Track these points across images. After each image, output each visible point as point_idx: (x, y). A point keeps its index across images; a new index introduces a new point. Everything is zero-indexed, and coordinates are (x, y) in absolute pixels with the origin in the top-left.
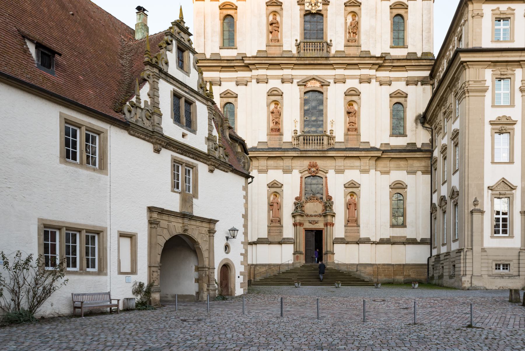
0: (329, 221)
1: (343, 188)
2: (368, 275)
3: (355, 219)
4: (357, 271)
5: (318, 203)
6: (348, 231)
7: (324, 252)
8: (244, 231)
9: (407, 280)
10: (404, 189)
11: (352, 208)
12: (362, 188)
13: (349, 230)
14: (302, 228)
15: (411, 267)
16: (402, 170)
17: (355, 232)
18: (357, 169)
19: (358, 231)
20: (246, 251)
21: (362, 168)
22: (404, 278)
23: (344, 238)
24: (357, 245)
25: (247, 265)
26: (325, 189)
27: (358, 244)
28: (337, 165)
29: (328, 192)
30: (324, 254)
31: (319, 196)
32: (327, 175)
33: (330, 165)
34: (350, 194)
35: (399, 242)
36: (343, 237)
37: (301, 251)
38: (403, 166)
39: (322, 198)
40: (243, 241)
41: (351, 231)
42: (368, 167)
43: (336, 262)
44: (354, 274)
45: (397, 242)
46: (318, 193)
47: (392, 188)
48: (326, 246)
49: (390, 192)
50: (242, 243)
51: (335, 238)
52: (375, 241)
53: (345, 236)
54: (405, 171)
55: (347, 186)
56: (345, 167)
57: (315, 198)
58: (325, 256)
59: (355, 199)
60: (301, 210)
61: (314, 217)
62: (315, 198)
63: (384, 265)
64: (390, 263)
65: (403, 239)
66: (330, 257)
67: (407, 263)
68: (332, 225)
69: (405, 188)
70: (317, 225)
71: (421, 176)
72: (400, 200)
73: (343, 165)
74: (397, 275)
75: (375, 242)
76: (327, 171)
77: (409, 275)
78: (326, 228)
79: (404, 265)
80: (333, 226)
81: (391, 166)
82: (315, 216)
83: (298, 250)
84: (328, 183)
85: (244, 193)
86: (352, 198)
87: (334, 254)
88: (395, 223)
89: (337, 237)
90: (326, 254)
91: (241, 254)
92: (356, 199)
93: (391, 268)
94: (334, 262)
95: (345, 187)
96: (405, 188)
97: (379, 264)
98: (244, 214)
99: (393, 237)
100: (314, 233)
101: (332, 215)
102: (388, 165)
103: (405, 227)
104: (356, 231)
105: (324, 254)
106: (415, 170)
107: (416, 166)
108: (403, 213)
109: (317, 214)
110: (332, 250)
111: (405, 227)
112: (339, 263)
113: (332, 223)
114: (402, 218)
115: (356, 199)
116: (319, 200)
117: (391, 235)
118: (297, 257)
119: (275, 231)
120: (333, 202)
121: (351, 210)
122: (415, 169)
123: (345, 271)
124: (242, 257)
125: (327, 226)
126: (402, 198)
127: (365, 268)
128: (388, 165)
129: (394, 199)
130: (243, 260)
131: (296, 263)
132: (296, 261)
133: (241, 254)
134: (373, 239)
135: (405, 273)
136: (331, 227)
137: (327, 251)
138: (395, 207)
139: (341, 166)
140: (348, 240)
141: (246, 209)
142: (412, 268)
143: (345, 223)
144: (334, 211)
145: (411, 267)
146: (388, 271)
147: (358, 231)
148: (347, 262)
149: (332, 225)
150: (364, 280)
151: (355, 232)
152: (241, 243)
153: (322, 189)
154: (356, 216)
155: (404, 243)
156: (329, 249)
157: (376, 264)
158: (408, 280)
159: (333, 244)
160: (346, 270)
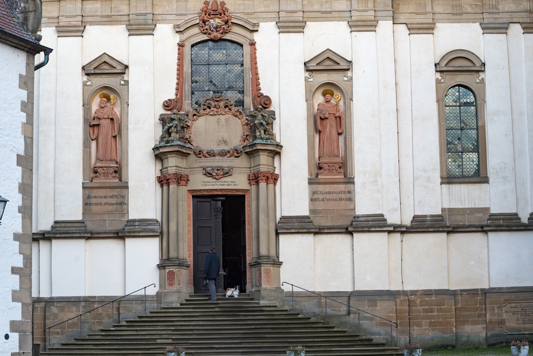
0: (263, 169)
1: (302, 74)
2: (382, 324)
3: (339, 160)
4: (349, 314)
5: (229, 116)
6: (321, 197)
7: (249, 260)
8: (20, 203)
9: (493, 336)
10: (476, 75)
11: (330, 127)
12: (357, 72)
13: (321, 193)
14: (183, 190)
15: (507, 297)
16: (468, 21)
17: (341, 199)
18: (340, 19)
19: (348, 196)
20: (28, 260)
21: (356, 16)
22: (487, 328)
23: (308, 216)
24: (346, 238)
25: (29, 301)
26: (248, 76)
27: (351, 233)
28: (282, 9)
29: (258, 84)
30: (251, 266)
31: (232, 96)
32: (256, 37)
33: (263, 9)
34: (321, 90)
35: (469, 226)
36: (306, 213)
37: (181, 256)
38: (469, 10)
39: (240, 103)
40: (20, 230)
41: (328, 196)
42: (372, 13)
43: (286, 288)
44: (342, 324)
45: (463, 227)
46: (230, 88)
47: (441, 72)
48: (254, 242)
49: (438, 82)
50: (17, 237)
51: (283, 218)
52: (399, 223)
53: (312, 211)
54: (477, 26)
55: (313, 66)
56: (306, 15)
57: (222, 104)
58: (254, 270)
59: (337, 105)
60: (182, 138)
61: (217, 158)
62: (222, 104)
63: (428, 293)
64: (445, 287)
65: (480, 215)
66: (268, 272)
67: (495, 284)
68: (271, 181)
69: (478, 71)
70: (228, 179)
71: (523, 36)
72: (467, 104)
73: (300, 7)
74: (465, 322)
75: (401, 226)
76: (254, 25)
77: (502, 322)
78: (254, 188)
79: (485, 292)
80: (275, 184)
81: (437, 9)
82: (223, 154)
83: (173, 254)
84: (258, 60)
85: (23, 94)
86: (328, 102)
87: (280, 264)
88: (457, 172)
89: (286, 214)
90: (257, 264)
91: (14, 270)
92: (341, 103)
93: (449, 303)
94: (279, 290)
95: (307, 70)
96: (478, 71)
97: (414, 293)
98: (22, 153)
99: (451, 211)
100: (219, 204)
101: (271, 151)
102: (429, 9)
103: (485, 180)
104: (343, 196)
105: (251, 266)
106: (505, 20)
107: (506, 9)
108: (477, 141)
109: (227, 148)
110: (273, 253)
111: (485, 180)
112: (296, 289)
113: (273, 174)
114: (474, 156)
115: (341, 103)
116: (234, 109)
117: (446, 206)
118: (171, 275)
119: (104, 201)
120: (273, 113)
121: (326, 135)
122: (505, 18)
123: (315, 315)
124: (17, 277)
125: (257, 183)
126: (472, 99)
127: (373, 303)
128: (429, 9)
129: (449, 100)
130: (17, 288)
131: (166, 294)
132: (169, 289)
133: (14, 270)
134: (393, 219)
135: (488, 316)
136: (271, 186)
137: (259, 257)
138: (455, 124)
139: (295, 12)
140: (320, 221)
141: (29, 141)
142: (508, 301)
143: (310, 174)
144: (278, 140)
145: (507, 297)
146: (440, 310)
147: (348, 196)
148: (319, 288)
149: (271, 181)
150: (371, 340)
151: (341, 199)
152: (11, 237)
153: (241, 76)
154: (342, 152)
155: (483, 229)
156: (263, 251)
157: (404, 293)
158: (498, 335)
159: (277, 234)
160: (317, 310)
